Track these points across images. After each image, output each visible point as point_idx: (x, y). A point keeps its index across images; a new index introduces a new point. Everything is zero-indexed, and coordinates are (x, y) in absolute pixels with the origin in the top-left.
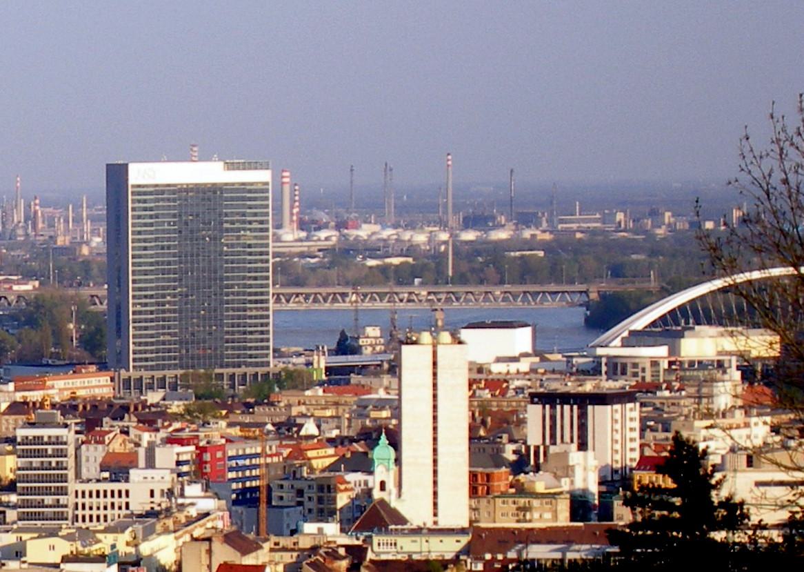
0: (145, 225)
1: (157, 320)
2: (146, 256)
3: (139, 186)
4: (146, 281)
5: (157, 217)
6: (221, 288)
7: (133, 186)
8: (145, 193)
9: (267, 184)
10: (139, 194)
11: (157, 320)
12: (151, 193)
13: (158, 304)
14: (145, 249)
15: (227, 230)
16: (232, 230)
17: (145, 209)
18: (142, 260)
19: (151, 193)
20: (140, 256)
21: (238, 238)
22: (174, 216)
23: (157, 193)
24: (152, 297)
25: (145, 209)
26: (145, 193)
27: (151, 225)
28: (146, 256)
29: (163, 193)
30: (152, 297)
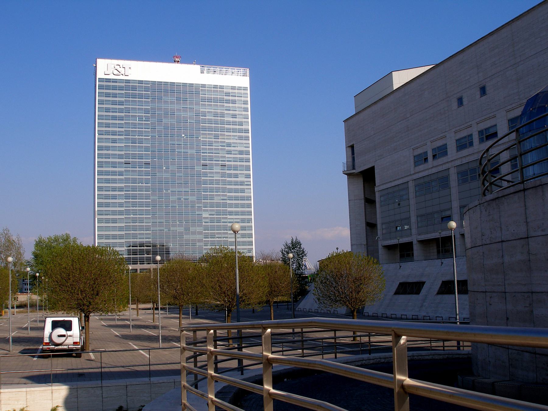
0: (114, 118)
1: (128, 212)
2: (114, 148)
3: (108, 80)
4: (114, 173)
5: (128, 110)
6: (199, 183)
7: (101, 80)
8: (114, 88)
9: (245, 89)
10: (108, 88)
11: (128, 212)
12: (121, 88)
13: (127, 197)
14: (114, 141)
15: (204, 129)
16: (210, 129)
17: (114, 103)
18: (110, 152)
19: (121, 88)
20: (108, 148)
21: (216, 137)
22: (146, 111)
23: (127, 88)
24: (121, 189)
25: (114, 103)
26: (114, 88)
27: (121, 119)
28: (114, 148)
29: (134, 88)
30: (121, 189)
